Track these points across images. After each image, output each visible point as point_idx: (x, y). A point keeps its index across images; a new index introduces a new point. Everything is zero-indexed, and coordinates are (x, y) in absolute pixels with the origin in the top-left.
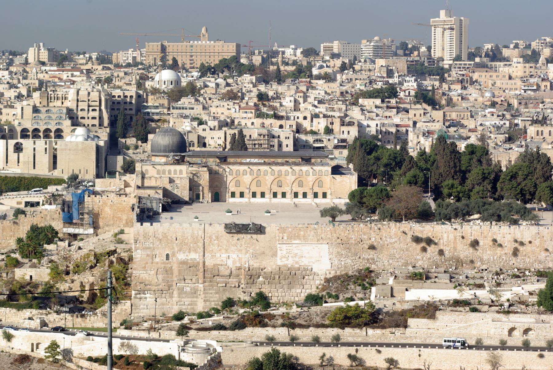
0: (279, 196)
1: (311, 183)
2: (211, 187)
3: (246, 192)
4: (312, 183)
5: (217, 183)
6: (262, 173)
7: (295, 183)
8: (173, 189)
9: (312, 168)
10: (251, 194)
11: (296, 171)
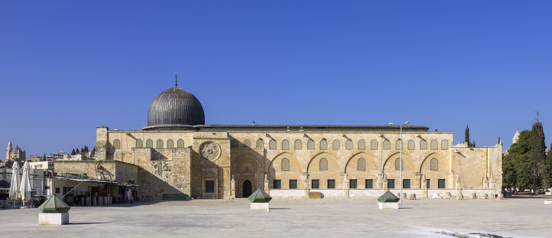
0: (361, 185)
1: (418, 163)
2: (235, 171)
3: (302, 179)
4: (419, 163)
5: (247, 164)
6: (330, 146)
7: (388, 163)
8: (160, 172)
9: (419, 137)
10: (310, 183)
11: (391, 140)
